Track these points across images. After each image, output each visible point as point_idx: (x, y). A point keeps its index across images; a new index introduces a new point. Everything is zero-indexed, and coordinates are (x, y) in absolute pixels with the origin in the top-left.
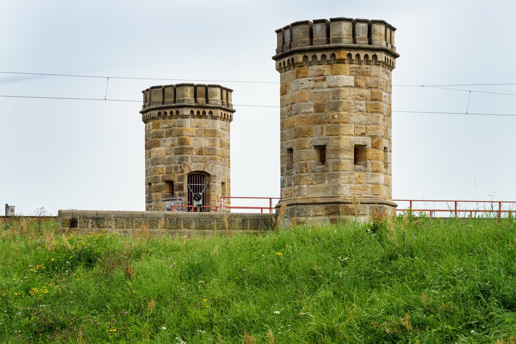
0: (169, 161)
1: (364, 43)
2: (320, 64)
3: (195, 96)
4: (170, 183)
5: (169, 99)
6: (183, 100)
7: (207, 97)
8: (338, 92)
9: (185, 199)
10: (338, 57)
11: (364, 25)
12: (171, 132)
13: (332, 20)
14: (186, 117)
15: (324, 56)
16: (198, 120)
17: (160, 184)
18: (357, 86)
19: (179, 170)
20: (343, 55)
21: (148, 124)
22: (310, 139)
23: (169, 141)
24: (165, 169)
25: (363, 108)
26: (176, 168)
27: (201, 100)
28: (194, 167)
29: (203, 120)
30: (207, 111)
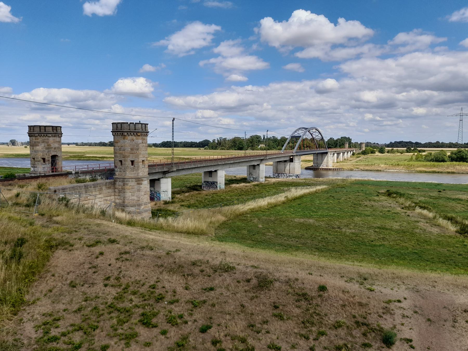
0: (43, 152)
1: (144, 130)
2: (132, 136)
3: (53, 130)
4: (44, 159)
5: (43, 131)
6: (49, 131)
7: (56, 130)
8: (138, 145)
9: (50, 165)
10: (138, 134)
11: (144, 125)
12: (44, 141)
13: (136, 123)
14: (50, 137)
15: (133, 134)
16: (54, 138)
17: (40, 159)
18: (142, 143)
19: (48, 155)
20: (139, 134)
21: (31, 138)
22: (129, 158)
23: (43, 145)
24: (41, 154)
25: (144, 149)
26: (46, 154)
27: (55, 131)
28: (53, 154)
29: (55, 138)
30: (57, 135)
